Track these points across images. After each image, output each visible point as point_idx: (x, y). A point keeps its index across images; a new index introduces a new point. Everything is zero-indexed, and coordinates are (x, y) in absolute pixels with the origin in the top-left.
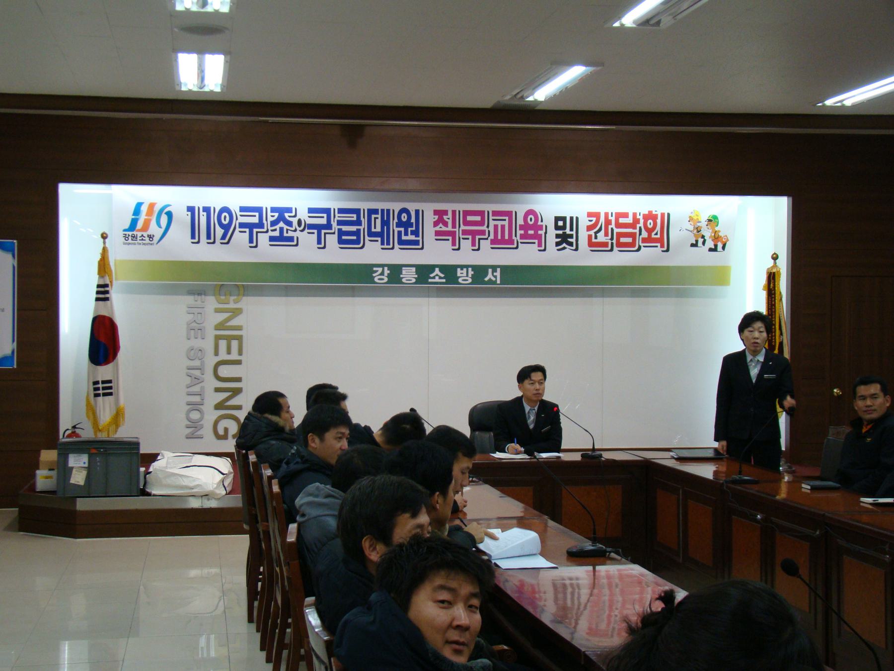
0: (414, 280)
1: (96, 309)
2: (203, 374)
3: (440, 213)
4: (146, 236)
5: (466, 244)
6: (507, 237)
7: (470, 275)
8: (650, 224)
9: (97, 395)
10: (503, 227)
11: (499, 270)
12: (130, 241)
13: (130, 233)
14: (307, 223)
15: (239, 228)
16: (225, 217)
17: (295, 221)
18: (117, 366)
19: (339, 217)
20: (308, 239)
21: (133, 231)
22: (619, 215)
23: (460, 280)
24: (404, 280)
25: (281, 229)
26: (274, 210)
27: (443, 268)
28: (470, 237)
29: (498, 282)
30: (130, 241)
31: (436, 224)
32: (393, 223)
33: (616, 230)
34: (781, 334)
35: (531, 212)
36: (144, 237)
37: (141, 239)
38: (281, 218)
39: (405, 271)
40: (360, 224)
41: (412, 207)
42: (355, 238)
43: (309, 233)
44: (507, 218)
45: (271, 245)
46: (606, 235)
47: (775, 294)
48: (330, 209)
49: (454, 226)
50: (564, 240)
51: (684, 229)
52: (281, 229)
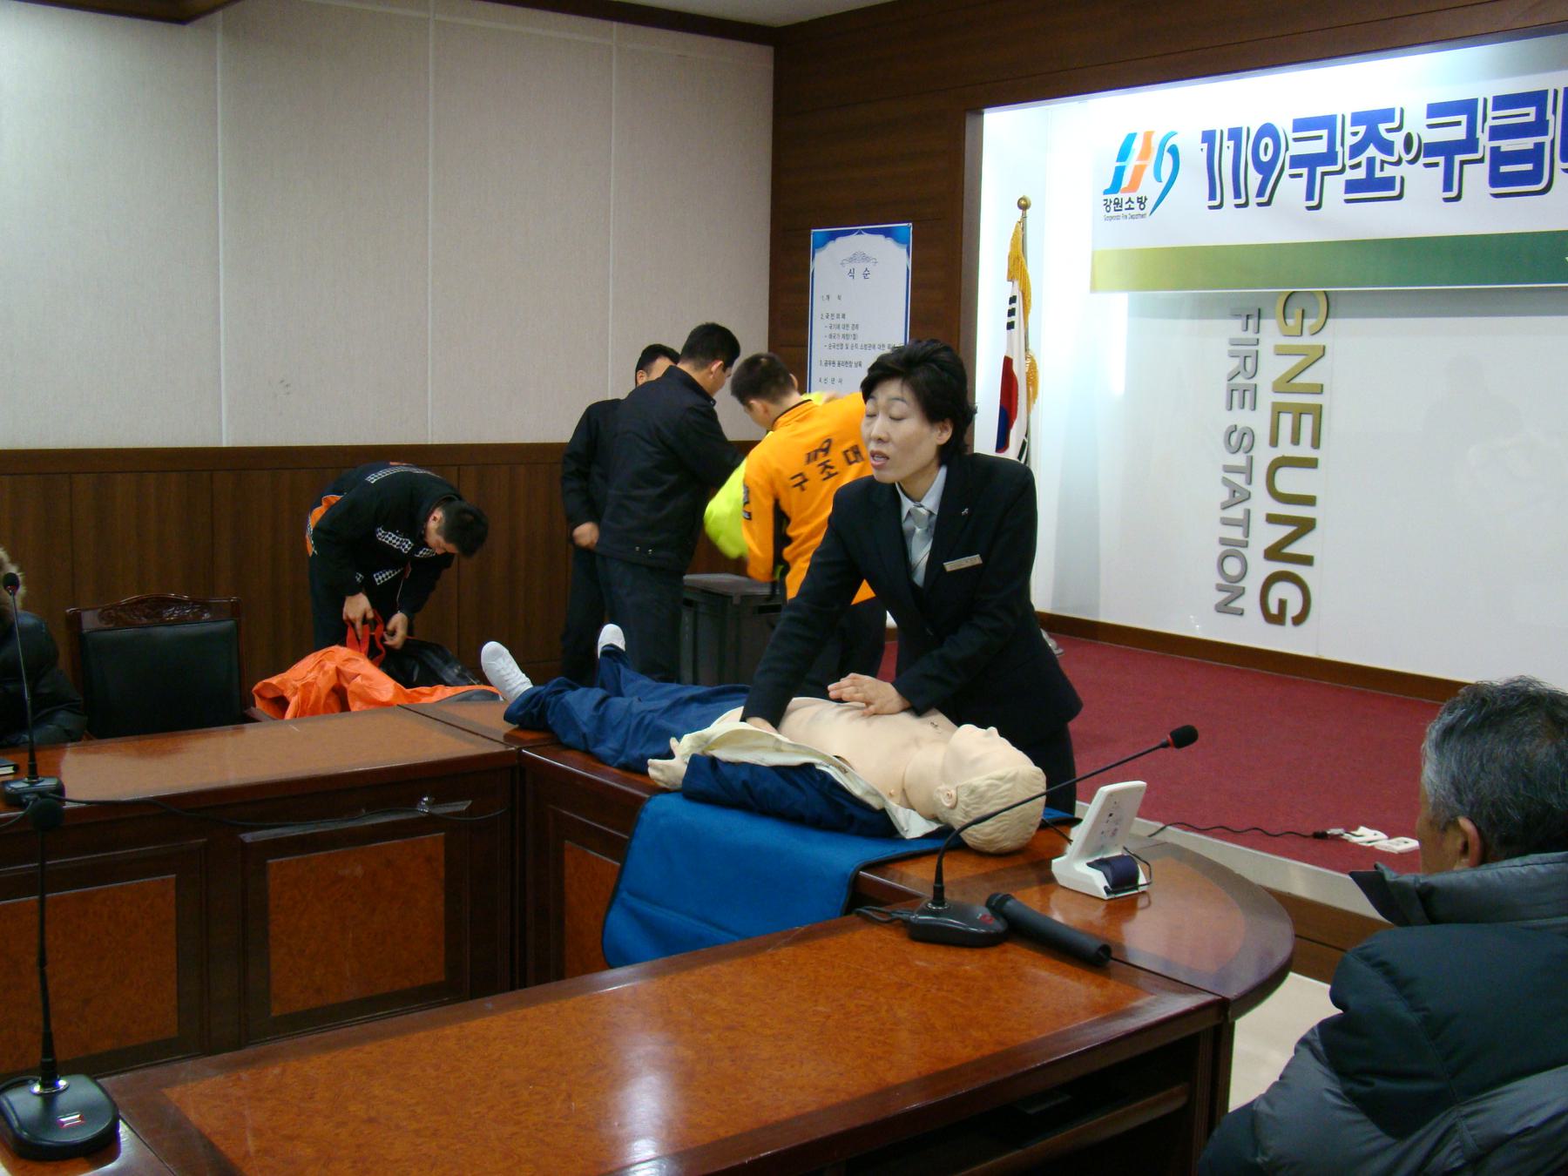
4: (1134, 199)
12: (1113, 213)
13: (1112, 197)
15: (1292, 167)
16: (1266, 146)
17: (1398, 139)
19: (1494, 118)
20: (1423, 180)
21: (1116, 193)
25: (1371, 161)
26: (1358, 119)
36: (1133, 203)
37: (1127, 206)
38: (1373, 137)
40: (1545, 133)
42: (1529, 167)
43: (1427, 165)
45: (1348, 201)
48: (1475, 101)
52: (1371, 161)
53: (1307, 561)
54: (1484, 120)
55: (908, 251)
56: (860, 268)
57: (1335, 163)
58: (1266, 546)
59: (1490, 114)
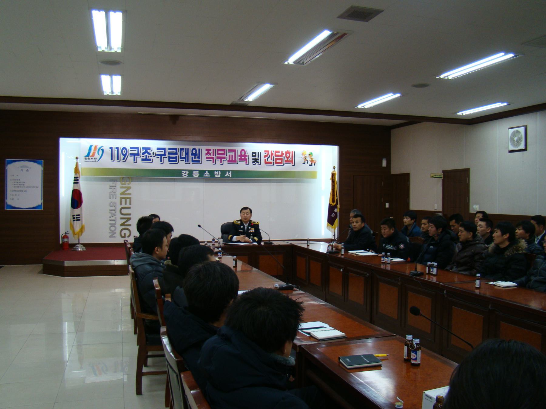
0: (198, 176)
1: (74, 187)
2: (116, 212)
3: (208, 150)
5: (218, 162)
6: (234, 160)
7: (220, 174)
8: (288, 155)
9: (74, 221)
10: (232, 155)
11: (231, 172)
13: (87, 157)
14: (156, 153)
15: (130, 155)
16: (124, 151)
18: (82, 209)
20: (156, 160)
22: (276, 152)
23: (216, 176)
24: (194, 176)
25: (146, 156)
26: (143, 148)
27: (209, 171)
28: (220, 159)
29: (231, 177)
30: (87, 160)
31: (206, 154)
32: (190, 154)
33: (275, 157)
34: (337, 196)
35: (243, 150)
39: (194, 172)
40: (177, 154)
41: (197, 148)
42: (175, 159)
44: (234, 152)
46: (271, 159)
47: (334, 181)
49: (213, 155)
50: (255, 161)
51: (300, 157)
52: (146, 156)
53: (130, 225)
54: (167, 151)
55: (42, 166)
56: (25, 169)
57: (139, 155)
58: (120, 224)
59: (168, 150)
